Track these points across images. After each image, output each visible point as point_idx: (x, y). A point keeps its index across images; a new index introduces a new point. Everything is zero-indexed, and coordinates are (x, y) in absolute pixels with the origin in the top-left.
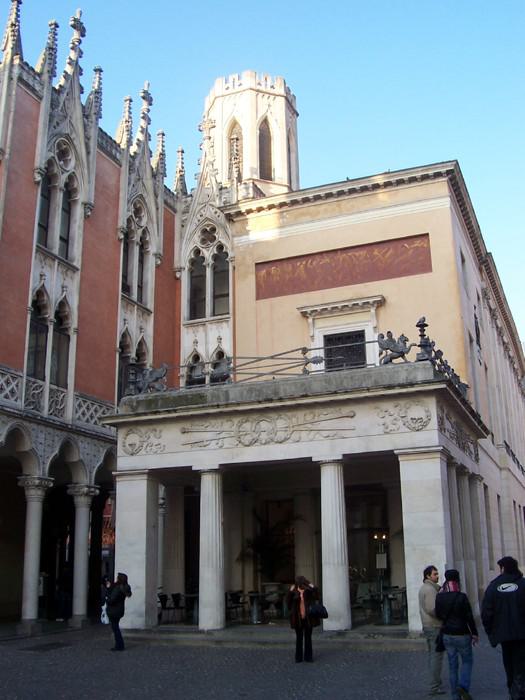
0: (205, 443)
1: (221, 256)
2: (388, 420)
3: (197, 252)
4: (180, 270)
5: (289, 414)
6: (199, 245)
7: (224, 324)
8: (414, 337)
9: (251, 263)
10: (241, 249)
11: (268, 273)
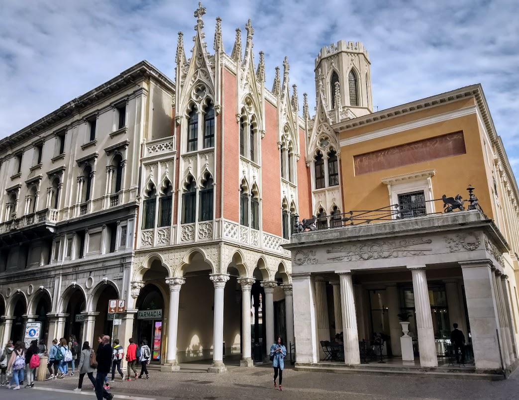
0: (341, 258)
1: (332, 154)
2: (452, 244)
3: (318, 152)
5: (390, 242)
6: (319, 147)
7: (337, 191)
8: (466, 196)
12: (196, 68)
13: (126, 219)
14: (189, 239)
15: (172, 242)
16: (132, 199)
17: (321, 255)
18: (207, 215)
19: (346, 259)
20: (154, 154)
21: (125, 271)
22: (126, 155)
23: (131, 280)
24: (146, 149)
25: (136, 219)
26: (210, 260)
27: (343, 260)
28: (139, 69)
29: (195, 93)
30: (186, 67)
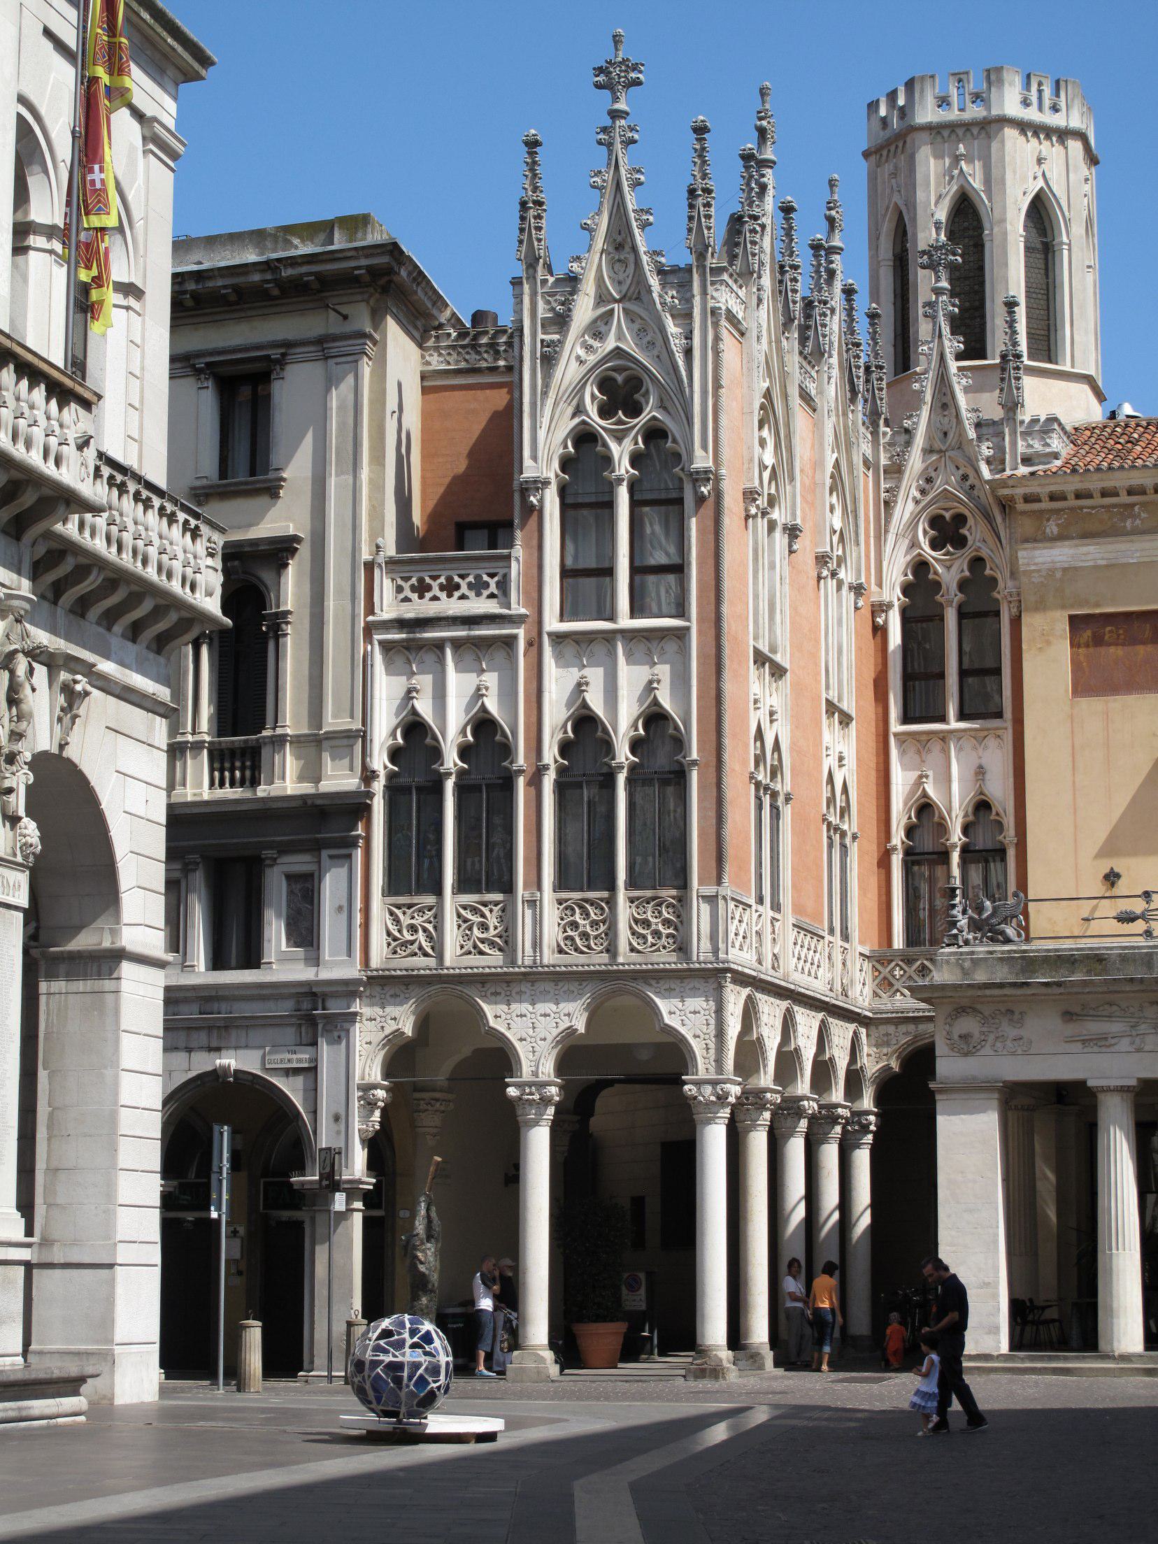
1: (978, 580)
3: (920, 567)
10: (1036, 579)
12: (602, 298)
13: (316, 847)
14: (589, 947)
15: (525, 955)
16: (339, 778)
17: (1042, 1026)
18: (664, 863)
19: (1124, 1045)
21: (325, 1048)
22: (291, 589)
23: (357, 1080)
24: (385, 587)
25: (359, 854)
26: (683, 1030)
27: (1116, 1048)
28: (364, 262)
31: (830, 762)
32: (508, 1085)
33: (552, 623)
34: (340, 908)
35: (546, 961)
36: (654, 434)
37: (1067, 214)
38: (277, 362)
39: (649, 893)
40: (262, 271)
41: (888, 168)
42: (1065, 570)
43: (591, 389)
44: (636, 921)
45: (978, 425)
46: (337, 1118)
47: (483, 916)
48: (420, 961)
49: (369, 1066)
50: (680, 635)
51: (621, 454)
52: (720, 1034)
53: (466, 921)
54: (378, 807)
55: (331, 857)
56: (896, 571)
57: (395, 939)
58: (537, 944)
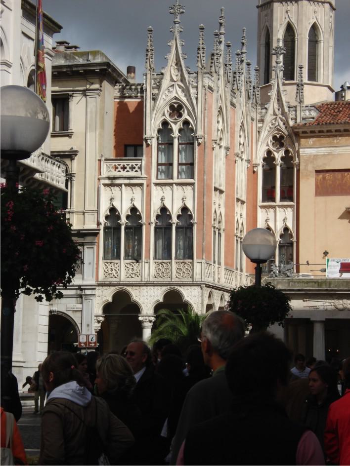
3: (269, 152)
4: (256, 166)
7: (289, 210)
9: (311, 168)
11: (324, 178)
14: (164, 276)
16: (91, 225)
20: (115, 174)
24: (104, 165)
29: (169, 110)
30: (159, 77)
31: (237, 217)
32: (139, 316)
33: (154, 180)
34: (90, 263)
35: (151, 280)
36: (186, 123)
37: (323, 30)
38: (71, 95)
39: (182, 261)
40: (67, 68)
41: (264, 13)
42: (314, 155)
43: (168, 108)
44: (178, 269)
45: (289, 107)
46: (88, 325)
47: (132, 266)
48: (114, 279)
49: (98, 311)
50: (192, 184)
51: (176, 128)
52: (202, 303)
53: (127, 268)
54: (102, 233)
55: (87, 248)
56: (261, 153)
57: (106, 273)
58: (149, 275)
